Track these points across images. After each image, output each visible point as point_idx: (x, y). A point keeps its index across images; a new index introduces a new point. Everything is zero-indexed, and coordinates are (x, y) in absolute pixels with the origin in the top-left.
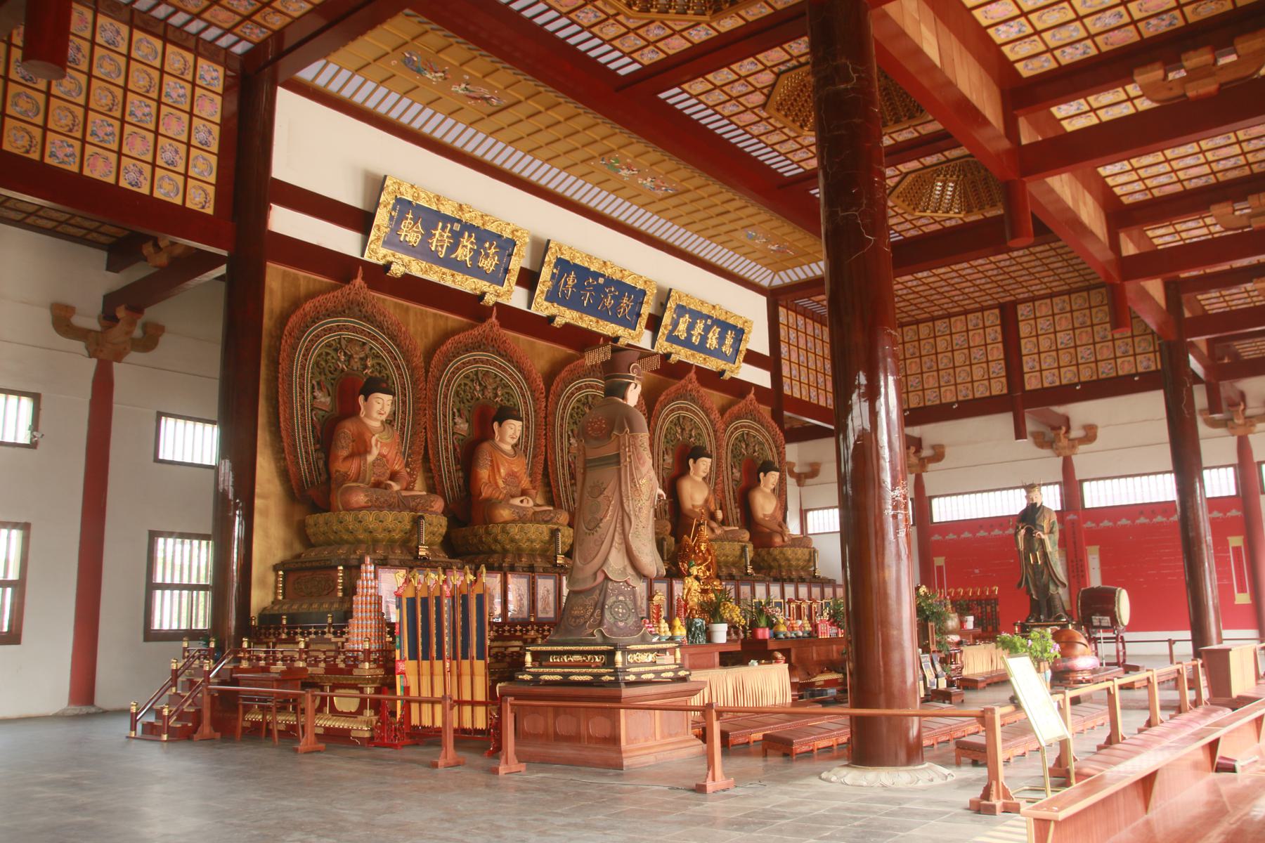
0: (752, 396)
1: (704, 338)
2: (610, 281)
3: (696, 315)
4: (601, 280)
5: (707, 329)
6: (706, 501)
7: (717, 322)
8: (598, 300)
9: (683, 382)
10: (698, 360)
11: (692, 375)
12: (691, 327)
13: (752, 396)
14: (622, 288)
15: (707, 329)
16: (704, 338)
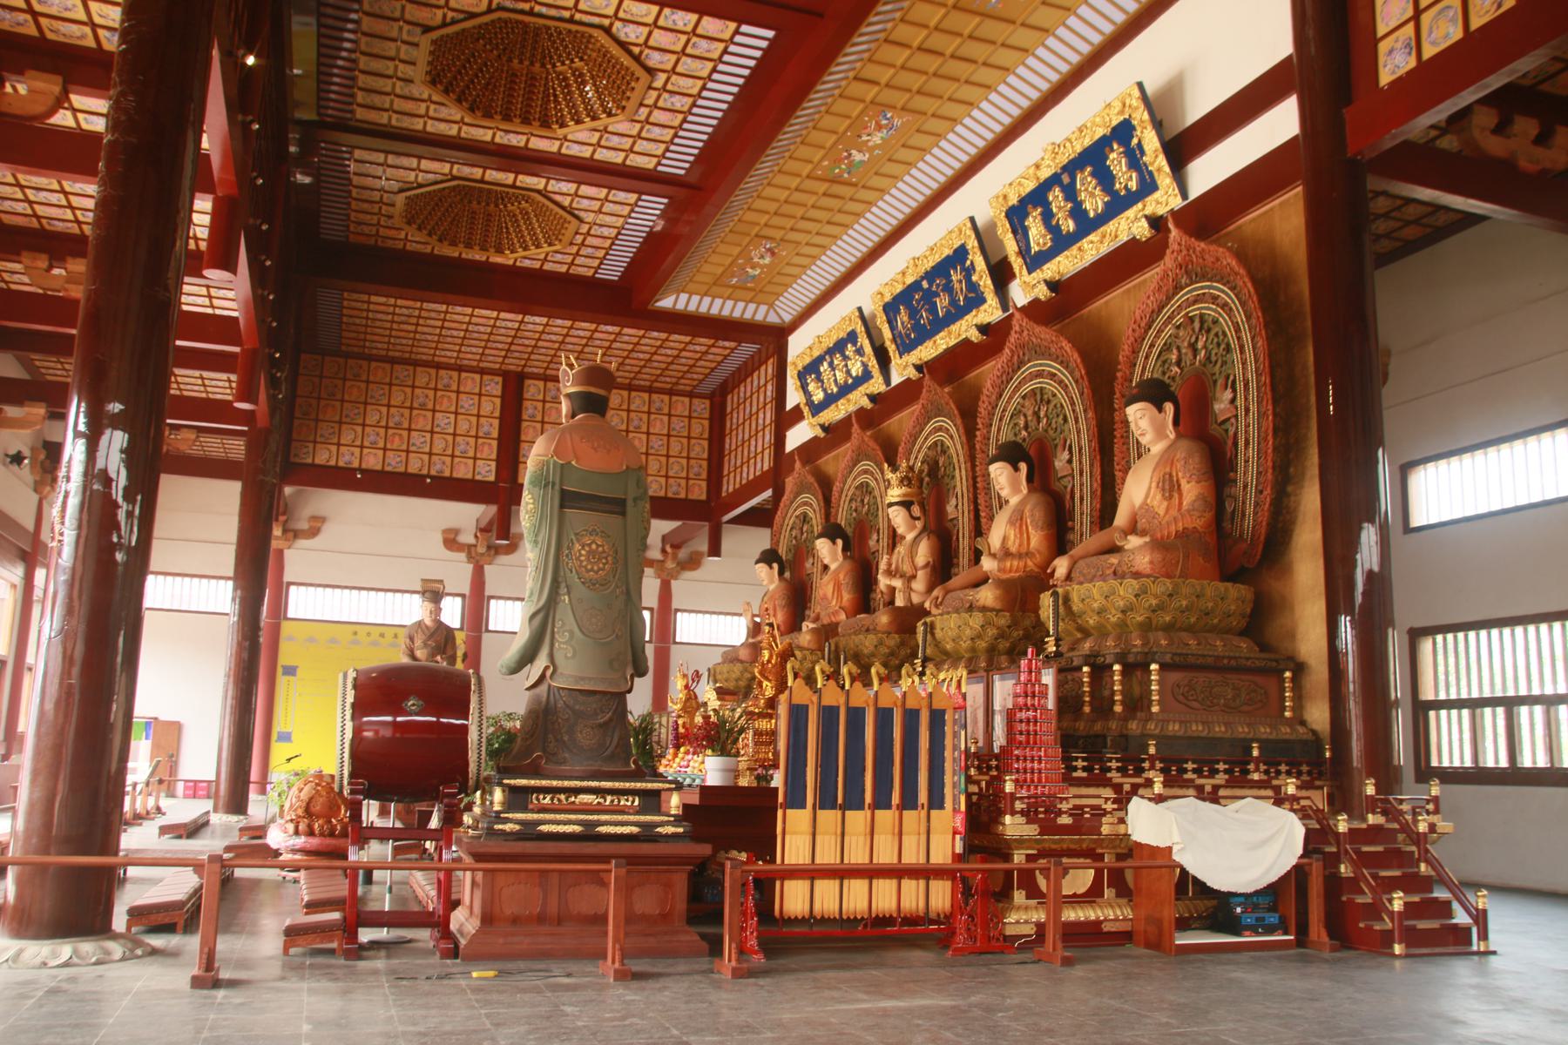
0: (1174, 232)
1: (1078, 212)
2: (930, 275)
3: (1038, 197)
4: (925, 284)
5: (1071, 193)
6: (1005, 539)
7: (1073, 167)
8: (933, 309)
9: (1013, 337)
10: (1092, 249)
11: (1017, 315)
12: (1047, 216)
13: (1174, 232)
14: (941, 270)
15: (1071, 193)
16: (1078, 212)
